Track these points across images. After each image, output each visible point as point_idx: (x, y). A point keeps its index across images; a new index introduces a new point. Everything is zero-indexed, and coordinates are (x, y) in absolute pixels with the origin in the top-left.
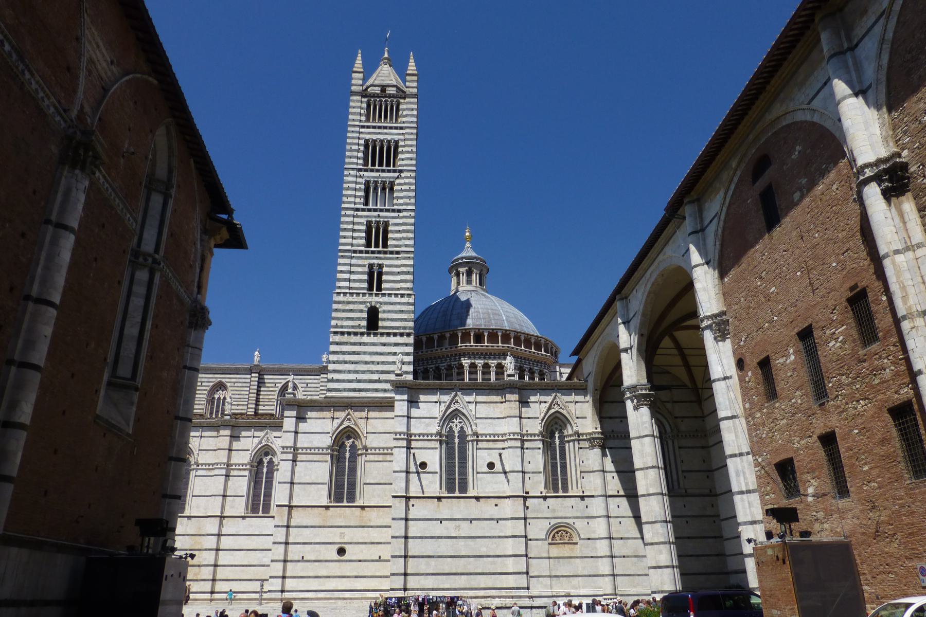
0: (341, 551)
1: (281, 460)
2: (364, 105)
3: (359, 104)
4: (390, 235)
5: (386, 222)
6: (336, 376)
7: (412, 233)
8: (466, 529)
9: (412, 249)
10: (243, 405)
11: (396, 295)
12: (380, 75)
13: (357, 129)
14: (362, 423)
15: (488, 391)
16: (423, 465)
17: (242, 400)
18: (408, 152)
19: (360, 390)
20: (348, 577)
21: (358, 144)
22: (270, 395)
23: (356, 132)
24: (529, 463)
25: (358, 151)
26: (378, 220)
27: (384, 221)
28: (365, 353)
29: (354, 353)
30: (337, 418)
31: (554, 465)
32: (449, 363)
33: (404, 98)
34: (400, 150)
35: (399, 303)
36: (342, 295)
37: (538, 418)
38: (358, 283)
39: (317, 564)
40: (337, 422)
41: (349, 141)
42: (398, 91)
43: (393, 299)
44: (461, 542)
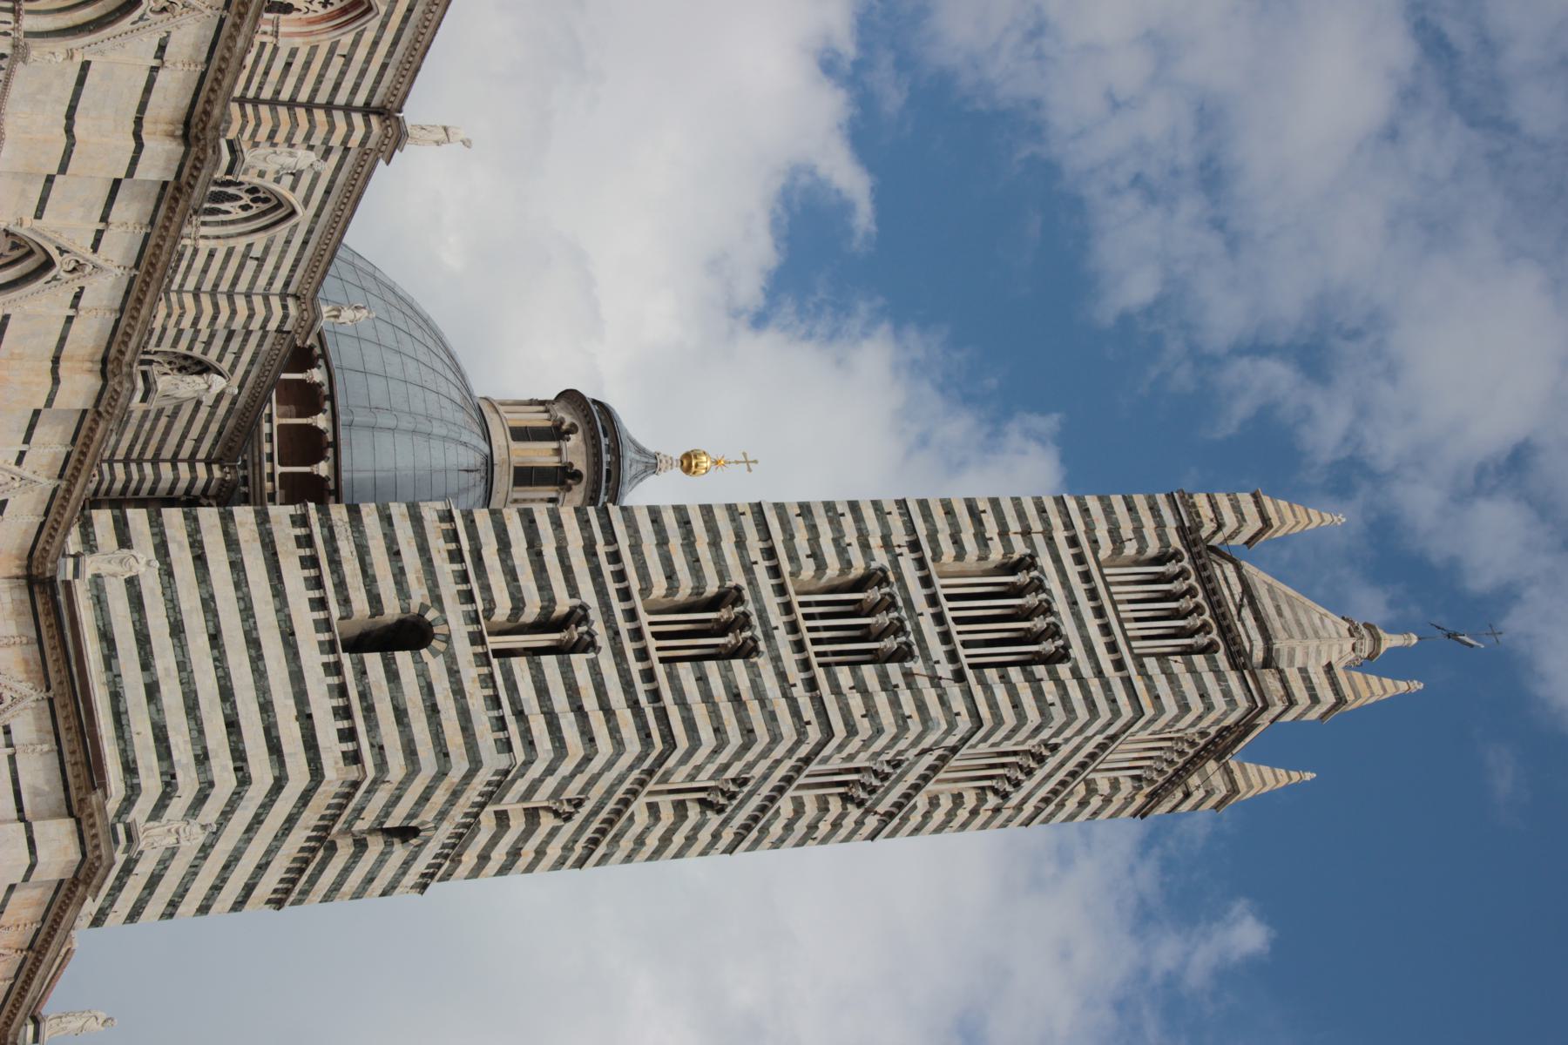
4: (711, 667)
5: (755, 651)
11: (495, 702)
13: (1056, 521)
18: (1038, 694)
21: (1004, 533)
23: (1046, 521)
26: (754, 620)
27: (754, 639)
33: (1234, 666)
34: (1040, 671)
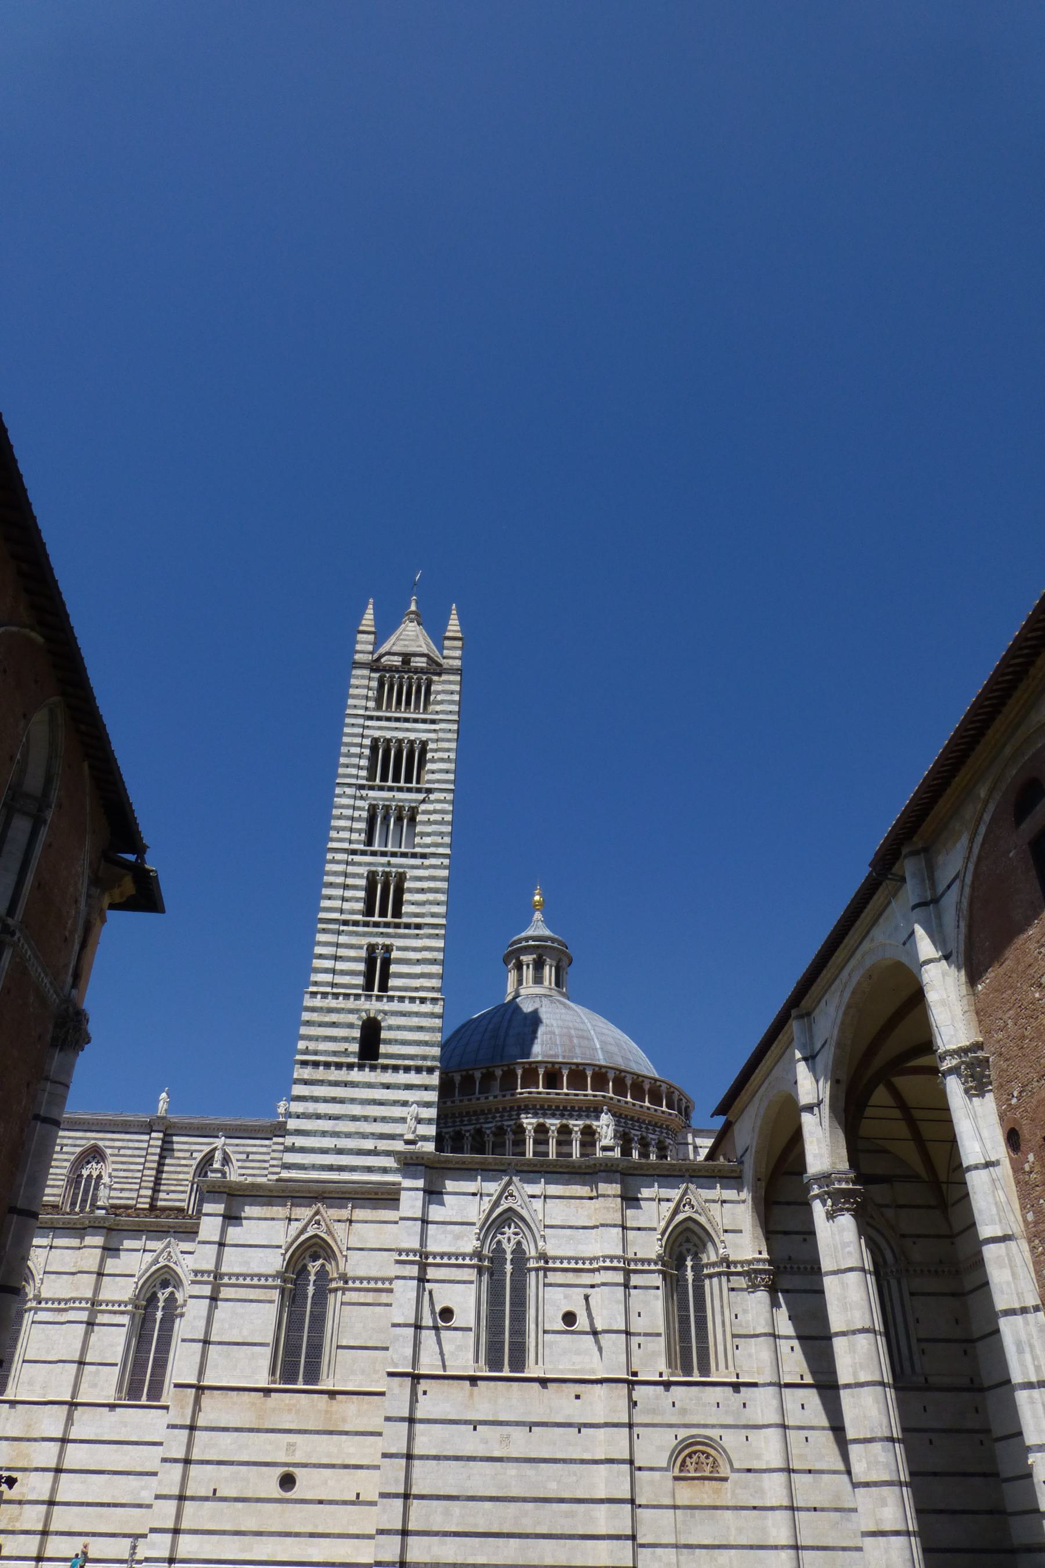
0: (287, 1481)
1: (191, 1297)
2: (374, 684)
3: (365, 682)
4: (407, 897)
6: (300, 1141)
7: (443, 893)
8: (520, 1443)
9: (443, 921)
10: (131, 1190)
11: (412, 1000)
12: (402, 637)
14: (340, 1229)
15: (566, 1176)
16: (447, 1313)
17: (130, 1180)
18: (442, 760)
19: (341, 1169)
20: (297, 1535)
21: (361, 746)
22: (179, 1173)
23: (359, 726)
24: (639, 1316)
25: (360, 756)
26: (387, 869)
27: (397, 873)
28: (353, 1101)
29: (334, 1100)
30: (297, 1220)
31: (684, 1321)
32: (499, 1124)
33: (439, 674)
34: (429, 756)
35: (417, 1014)
36: (319, 996)
37: (655, 1229)
38: (348, 977)
39: (240, 1505)
40: (296, 1226)
41: (345, 739)
42: (430, 662)
43: (407, 1006)
44: (512, 1469)
